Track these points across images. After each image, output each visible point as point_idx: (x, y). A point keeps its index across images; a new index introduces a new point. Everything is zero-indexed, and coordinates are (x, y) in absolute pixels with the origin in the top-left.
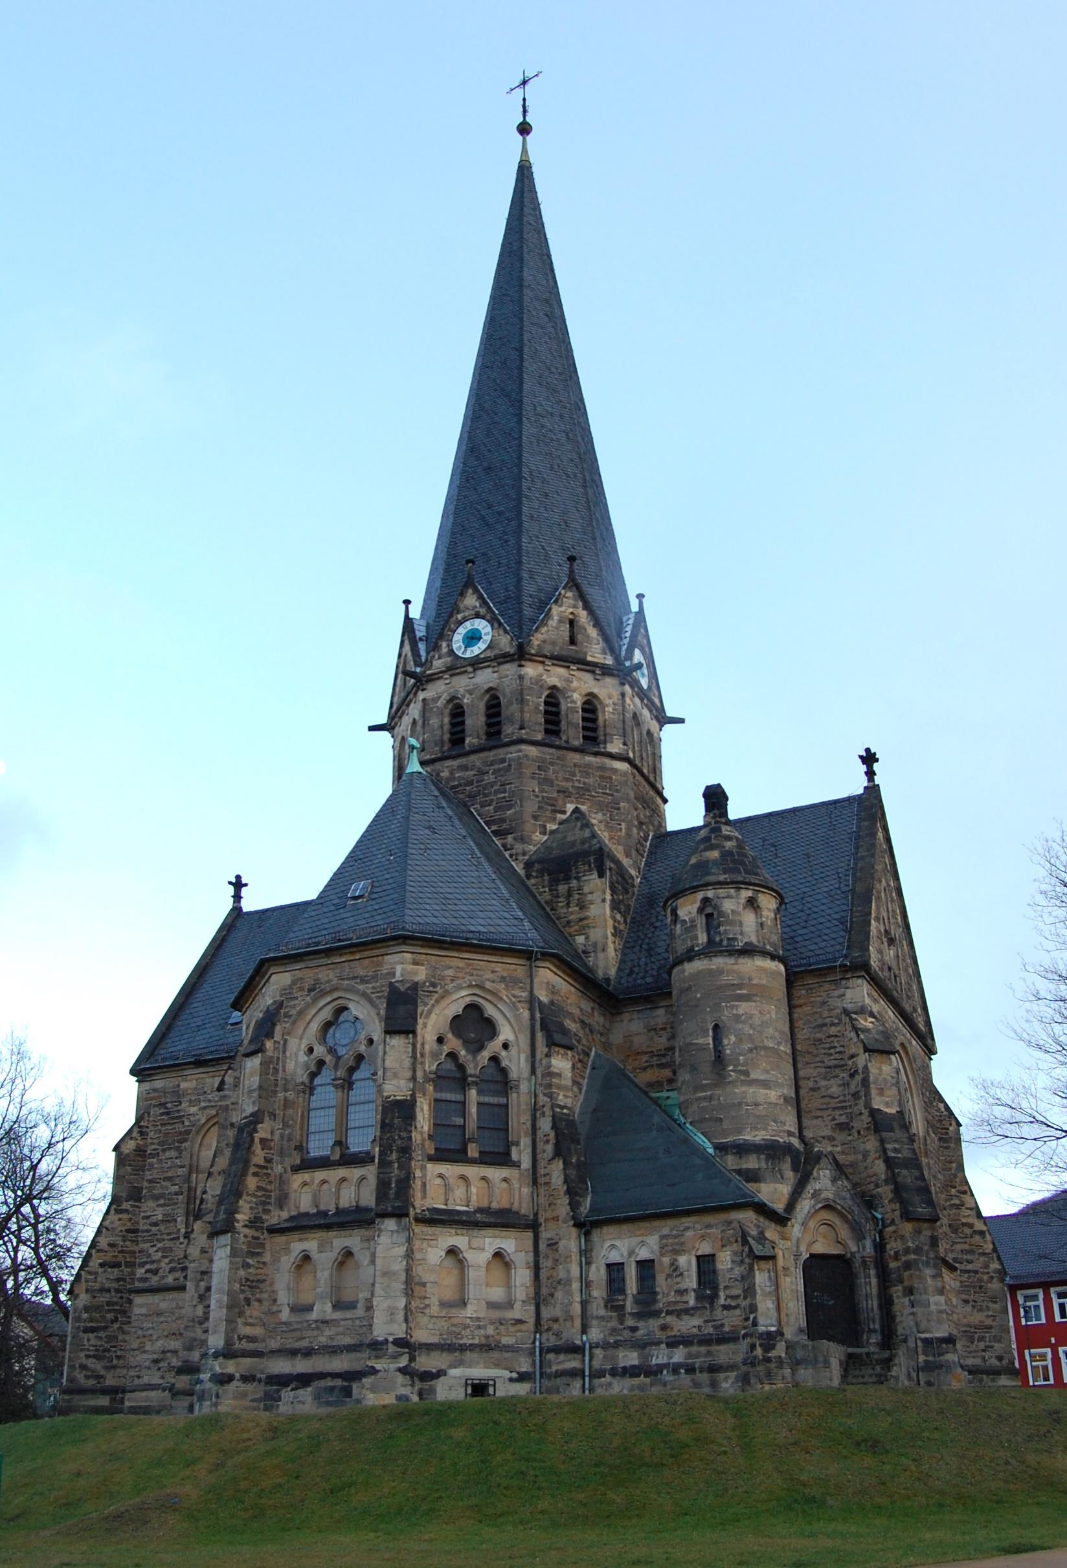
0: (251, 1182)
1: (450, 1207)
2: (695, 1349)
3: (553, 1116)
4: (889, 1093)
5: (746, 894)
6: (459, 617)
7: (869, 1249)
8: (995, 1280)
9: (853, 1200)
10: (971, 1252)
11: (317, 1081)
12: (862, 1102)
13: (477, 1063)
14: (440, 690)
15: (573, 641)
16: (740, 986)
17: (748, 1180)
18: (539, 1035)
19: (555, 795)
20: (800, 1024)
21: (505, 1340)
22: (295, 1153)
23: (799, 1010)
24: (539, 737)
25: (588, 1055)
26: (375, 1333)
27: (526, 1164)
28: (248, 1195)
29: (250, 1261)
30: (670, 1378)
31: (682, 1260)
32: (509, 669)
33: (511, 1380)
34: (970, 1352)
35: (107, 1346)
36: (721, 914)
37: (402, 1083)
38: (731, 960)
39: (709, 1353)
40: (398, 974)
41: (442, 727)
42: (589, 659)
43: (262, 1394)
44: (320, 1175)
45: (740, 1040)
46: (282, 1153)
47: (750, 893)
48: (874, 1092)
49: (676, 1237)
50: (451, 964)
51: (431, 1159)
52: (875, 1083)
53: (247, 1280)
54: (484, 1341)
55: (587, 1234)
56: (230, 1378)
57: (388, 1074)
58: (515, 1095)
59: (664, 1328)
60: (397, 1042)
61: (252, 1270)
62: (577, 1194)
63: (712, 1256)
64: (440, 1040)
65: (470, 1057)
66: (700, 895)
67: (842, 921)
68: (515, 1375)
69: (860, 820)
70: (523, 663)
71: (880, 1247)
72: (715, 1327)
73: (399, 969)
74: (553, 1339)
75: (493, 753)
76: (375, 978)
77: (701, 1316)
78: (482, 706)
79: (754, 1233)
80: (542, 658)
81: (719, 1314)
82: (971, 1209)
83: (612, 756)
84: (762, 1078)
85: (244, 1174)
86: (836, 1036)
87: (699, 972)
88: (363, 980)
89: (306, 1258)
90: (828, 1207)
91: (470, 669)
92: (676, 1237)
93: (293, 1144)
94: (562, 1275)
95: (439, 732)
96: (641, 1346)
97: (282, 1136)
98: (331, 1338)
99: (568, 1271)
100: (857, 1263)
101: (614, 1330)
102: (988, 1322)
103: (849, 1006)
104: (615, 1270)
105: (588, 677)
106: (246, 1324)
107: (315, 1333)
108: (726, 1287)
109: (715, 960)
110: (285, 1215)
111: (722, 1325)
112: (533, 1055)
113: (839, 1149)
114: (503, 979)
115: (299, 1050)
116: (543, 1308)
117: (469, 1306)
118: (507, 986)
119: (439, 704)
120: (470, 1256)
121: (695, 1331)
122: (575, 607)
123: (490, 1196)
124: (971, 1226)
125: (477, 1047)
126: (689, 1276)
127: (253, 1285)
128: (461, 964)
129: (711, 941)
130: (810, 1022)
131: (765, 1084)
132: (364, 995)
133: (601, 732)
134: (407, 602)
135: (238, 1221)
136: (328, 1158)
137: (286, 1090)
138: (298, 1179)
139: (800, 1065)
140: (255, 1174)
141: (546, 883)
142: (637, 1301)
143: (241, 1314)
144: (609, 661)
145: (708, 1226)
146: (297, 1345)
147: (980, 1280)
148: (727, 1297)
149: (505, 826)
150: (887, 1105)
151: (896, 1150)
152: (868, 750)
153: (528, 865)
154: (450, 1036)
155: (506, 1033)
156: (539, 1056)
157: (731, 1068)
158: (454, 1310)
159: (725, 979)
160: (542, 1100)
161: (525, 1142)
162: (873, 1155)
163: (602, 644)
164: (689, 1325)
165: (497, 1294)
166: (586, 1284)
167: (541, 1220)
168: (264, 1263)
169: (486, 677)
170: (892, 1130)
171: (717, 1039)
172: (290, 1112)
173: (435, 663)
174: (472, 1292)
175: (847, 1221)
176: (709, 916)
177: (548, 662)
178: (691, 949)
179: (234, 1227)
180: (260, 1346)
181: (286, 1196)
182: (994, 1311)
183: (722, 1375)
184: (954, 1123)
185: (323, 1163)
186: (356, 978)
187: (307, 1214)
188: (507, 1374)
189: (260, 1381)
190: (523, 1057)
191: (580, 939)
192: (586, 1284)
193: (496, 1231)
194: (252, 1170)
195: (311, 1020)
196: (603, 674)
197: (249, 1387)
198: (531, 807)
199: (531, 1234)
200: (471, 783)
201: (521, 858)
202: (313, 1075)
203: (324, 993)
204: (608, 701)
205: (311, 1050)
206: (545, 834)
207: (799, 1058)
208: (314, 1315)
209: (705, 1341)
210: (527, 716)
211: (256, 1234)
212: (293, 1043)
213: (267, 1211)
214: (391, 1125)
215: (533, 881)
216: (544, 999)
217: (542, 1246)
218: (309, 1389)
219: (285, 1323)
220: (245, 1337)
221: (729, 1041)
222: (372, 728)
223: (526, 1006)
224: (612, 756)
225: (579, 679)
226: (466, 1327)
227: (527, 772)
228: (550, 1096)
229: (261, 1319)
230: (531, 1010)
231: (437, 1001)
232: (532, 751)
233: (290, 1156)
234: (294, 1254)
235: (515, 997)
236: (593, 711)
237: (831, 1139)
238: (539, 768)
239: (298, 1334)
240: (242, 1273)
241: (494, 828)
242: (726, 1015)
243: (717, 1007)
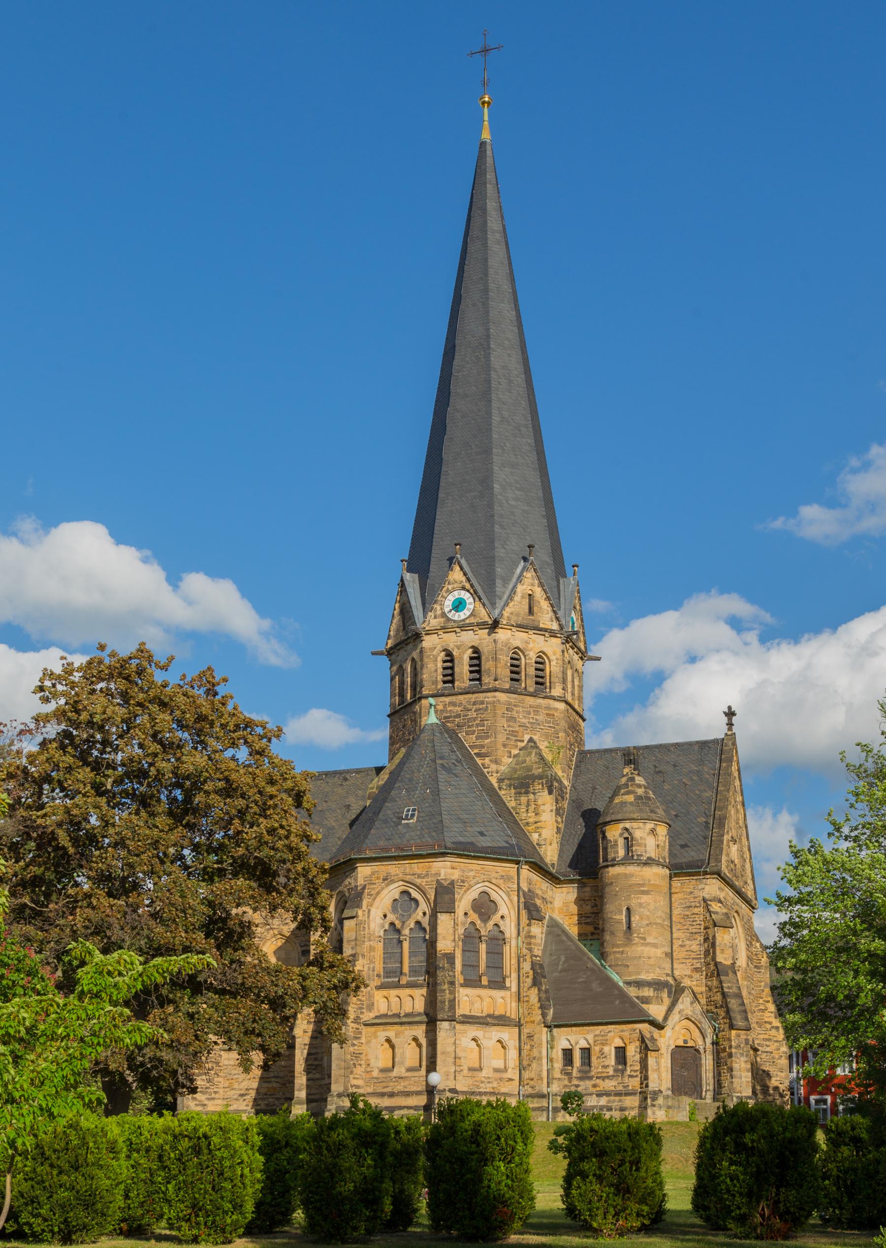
1: (473, 1014)
2: (612, 1098)
3: (532, 962)
5: (650, 825)
6: (450, 587)
10: (769, 1040)
13: (485, 929)
14: (435, 642)
15: (531, 611)
16: (643, 885)
17: (643, 1003)
18: (524, 914)
19: (517, 729)
22: (376, 978)
24: (507, 686)
27: (514, 989)
29: (355, 1042)
31: (606, 1049)
35: (208, 1085)
38: (638, 869)
39: (620, 1101)
42: (541, 626)
44: (393, 993)
47: (652, 826)
49: (603, 1036)
51: (462, 985)
54: (492, 1090)
58: (508, 947)
59: (595, 1086)
62: (546, 1008)
64: (466, 914)
65: (483, 925)
66: (621, 825)
72: (624, 1087)
73: (443, 872)
75: (476, 695)
76: (427, 875)
79: (648, 1036)
81: (626, 1079)
84: (653, 941)
87: (619, 874)
88: (419, 877)
90: (688, 1019)
91: (458, 630)
92: (603, 1036)
94: (535, 1053)
98: (405, 1087)
99: (540, 1052)
100: (702, 1051)
103: (707, 896)
109: (628, 867)
110: (372, 1015)
112: (519, 924)
113: (695, 983)
119: (434, 653)
120: (484, 1042)
121: (613, 1088)
122: (533, 585)
123: (495, 1006)
124: (770, 1023)
128: (478, 868)
131: (655, 946)
137: (370, 940)
139: (674, 930)
141: (513, 795)
142: (580, 1071)
143: (352, 1072)
144: (555, 626)
145: (622, 1031)
147: (773, 1058)
149: (483, 751)
151: (729, 988)
152: (730, 708)
153: (500, 781)
154: (471, 912)
155: (503, 910)
159: (634, 880)
161: (514, 975)
163: (551, 614)
164: (609, 1085)
165: (500, 1064)
166: (550, 1060)
167: (522, 1022)
170: (728, 975)
172: (372, 954)
173: (432, 621)
174: (485, 1063)
177: (514, 629)
178: (614, 859)
181: (373, 1004)
190: (513, 924)
192: (550, 1060)
198: (501, 738)
200: (459, 716)
201: (495, 775)
203: (393, 882)
204: (552, 657)
205: (385, 916)
206: (510, 757)
210: (499, 670)
212: (373, 911)
213: (362, 1013)
216: (526, 889)
217: (523, 1037)
221: (635, 919)
222: (373, 654)
224: (554, 698)
225: (534, 641)
226: (482, 1082)
227: (499, 712)
228: (530, 950)
231: (465, 892)
233: (374, 980)
237: (691, 977)
238: (507, 709)
239: (385, 1084)
241: (476, 751)
242: (633, 903)
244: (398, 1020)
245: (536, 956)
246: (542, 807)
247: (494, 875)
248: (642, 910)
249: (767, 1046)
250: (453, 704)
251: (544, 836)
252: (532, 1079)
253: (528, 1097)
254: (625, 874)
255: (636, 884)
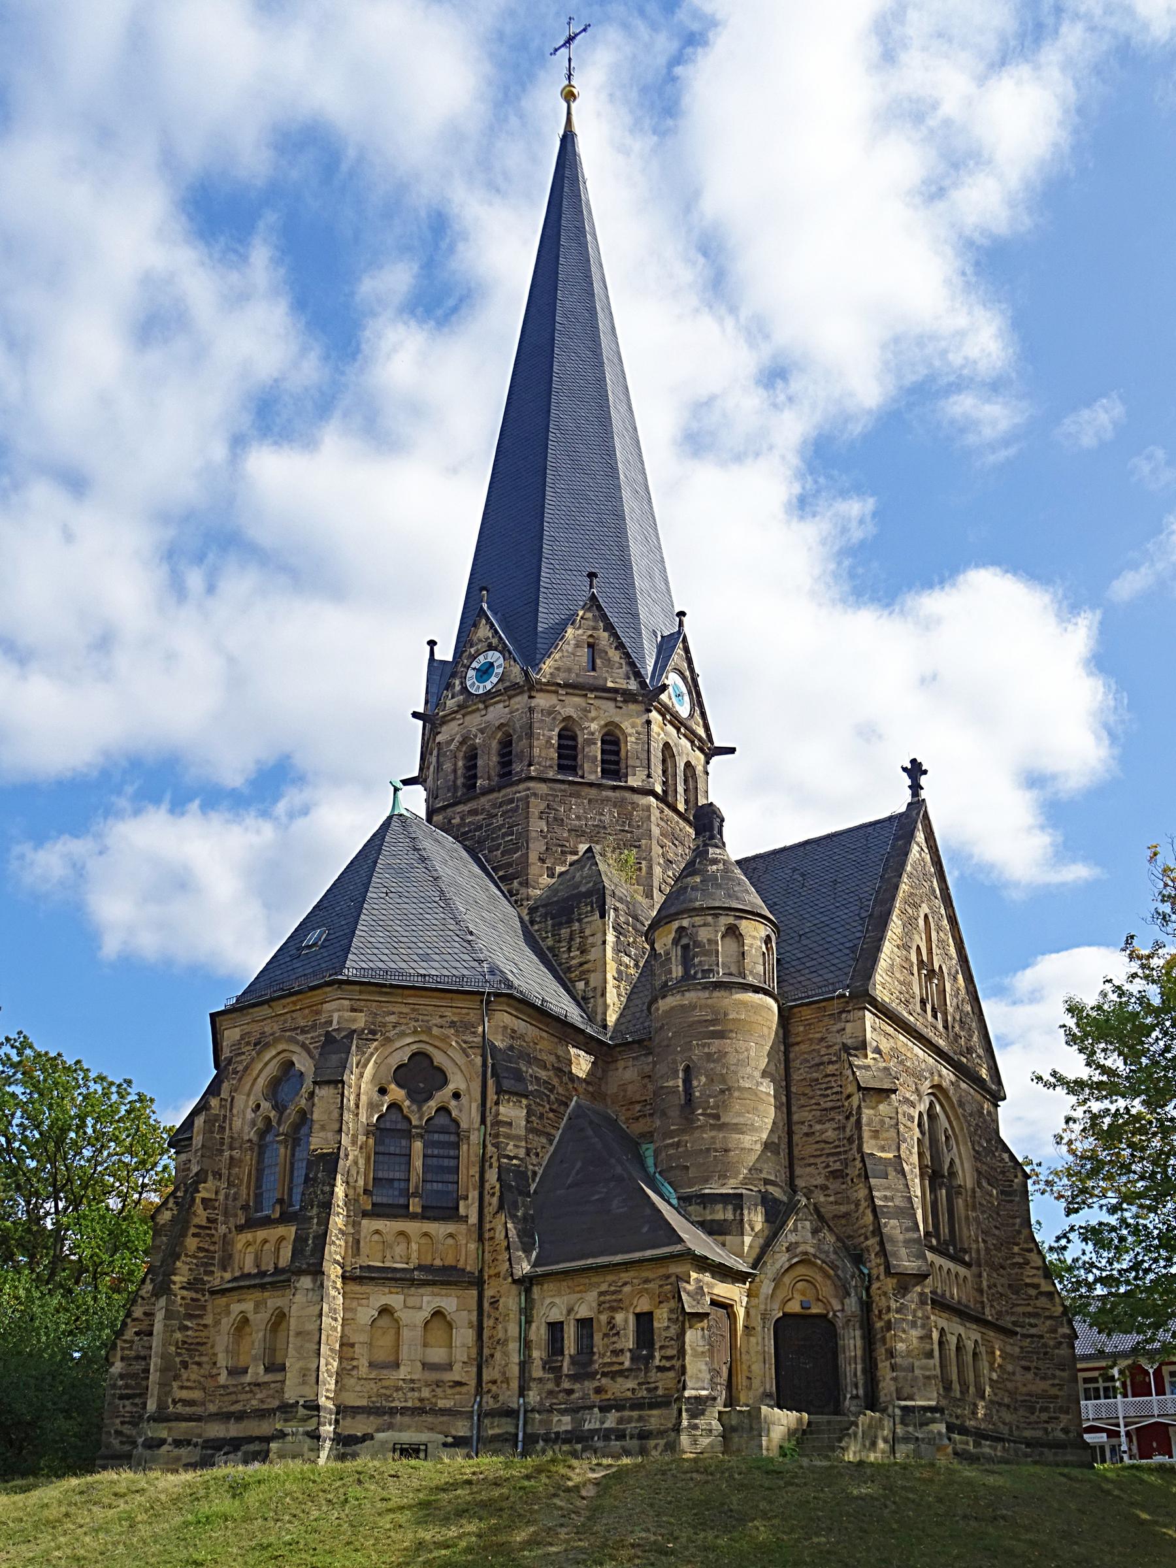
0: (191, 1243)
1: (387, 1264)
2: (626, 1413)
3: (499, 1168)
4: (885, 1135)
5: (725, 921)
6: (472, 651)
7: (852, 1304)
8: (1065, 1345)
9: (835, 1253)
10: (1036, 1315)
11: (269, 1138)
12: (855, 1146)
14: (454, 732)
16: (714, 1022)
20: (796, 1064)
21: (441, 1404)
22: (240, 1212)
23: (797, 1048)
25: (567, 1106)
26: (286, 1396)
27: (473, 1219)
28: (187, 1255)
29: (188, 1324)
30: (600, 1444)
31: (619, 1317)
32: (520, 701)
33: (445, 1445)
34: (1029, 1423)
36: (697, 944)
37: (330, 1135)
38: (707, 994)
40: (335, 1022)
41: (455, 771)
42: (610, 684)
43: (198, 1458)
44: (261, 1234)
45: (711, 1080)
46: (226, 1214)
48: (866, 1135)
49: (614, 1293)
50: (394, 1010)
51: (365, 1214)
52: (868, 1125)
53: (184, 1342)
54: (418, 1404)
55: (528, 1291)
56: (163, 1442)
57: (316, 1127)
59: (598, 1391)
60: (323, 1092)
61: (190, 1333)
63: (650, 1314)
65: (414, 1107)
67: (853, 949)
68: (450, 1440)
69: (896, 839)
70: (534, 694)
71: (866, 1306)
72: (648, 1390)
74: (491, 1401)
76: (314, 1027)
77: (636, 1377)
78: (494, 744)
80: (552, 687)
81: (654, 1375)
82: (1038, 1268)
83: (633, 790)
85: (183, 1235)
86: (834, 1075)
87: (672, 1008)
88: (303, 1032)
89: (244, 1321)
90: (806, 1261)
91: (481, 706)
92: (614, 1293)
93: (239, 1204)
94: (501, 1335)
95: (451, 777)
96: (574, 1410)
97: (227, 1196)
98: (262, 1402)
101: (551, 1393)
102: (1054, 1391)
103: (849, 1042)
104: (556, 1329)
105: (610, 705)
106: (182, 1388)
107: (249, 1396)
108: (662, 1348)
110: (228, 1276)
111: (656, 1388)
113: (832, 1199)
114: (453, 1024)
115: (246, 1106)
116: (484, 1370)
117: (402, 1368)
118: (457, 1031)
119: (452, 747)
120: (404, 1316)
121: (629, 1394)
124: (1036, 1286)
125: (420, 1096)
126: (626, 1335)
127: (194, 1349)
128: (405, 1010)
129: (687, 976)
130: (808, 1061)
132: (303, 1046)
133: (623, 765)
134: (432, 643)
135: (174, 1283)
136: (268, 1217)
137: (231, 1148)
138: (242, 1239)
139: (794, 1109)
140: (194, 1235)
144: (633, 685)
145: (647, 1281)
146: (233, 1408)
147: (1045, 1345)
148: (663, 1358)
149: (511, 871)
150: (883, 1149)
151: (886, 1198)
154: (393, 1086)
155: (456, 1082)
156: (488, 1106)
157: (700, 1111)
158: (385, 1372)
160: (490, 1149)
161: (474, 1195)
162: (864, 1204)
163: (625, 668)
164: (623, 1387)
166: (526, 1345)
168: (205, 1326)
169: (497, 713)
171: (687, 1081)
173: (448, 702)
174: (404, 1354)
175: (829, 1277)
176: (686, 948)
178: (665, 984)
179: (170, 1289)
180: (198, 1410)
181: (231, 1256)
182: (1062, 1379)
183: (652, 1443)
184: (1020, 1175)
185: (267, 1222)
186: (296, 1029)
187: (249, 1276)
188: (441, 1438)
189: (196, 1445)
190: (474, 1106)
191: (581, 985)
192: (526, 1345)
193: (436, 1290)
194: (193, 1230)
195: (258, 1076)
196: (625, 701)
197: (183, 1451)
199: (475, 1293)
201: (525, 903)
202: (262, 1134)
204: (629, 730)
205: (258, 1106)
206: (551, 876)
207: (793, 1101)
208: (248, 1378)
209: (637, 1405)
210: (536, 751)
211: (194, 1295)
212: (240, 1099)
214: (315, 1179)
215: (536, 927)
217: (486, 1305)
218: (240, 1454)
219: (223, 1387)
220: (180, 1400)
223: (479, 1051)
225: (598, 708)
226: (398, 1389)
229: (200, 1383)
230: (484, 1057)
232: (542, 788)
233: (236, 1215)
234: (233, 1316)
235: (465, 1042)
236: (617, 743)
237: (824, 1188)
239: (233, 1397)
240: (178, 1335)
241: (501, 873)
243: (688, 1047)
244: (257, 1281)
245: (510, 1158)
246: (590, 940)
247: (438, 1021)
248: (712, 1065)
249: (1031, 1325)
250: (474, 812)
251: (592, 984)
252: (494, 1382)
253: (487, 1415)
254: (682, 1006)
255: (700, 1022)
